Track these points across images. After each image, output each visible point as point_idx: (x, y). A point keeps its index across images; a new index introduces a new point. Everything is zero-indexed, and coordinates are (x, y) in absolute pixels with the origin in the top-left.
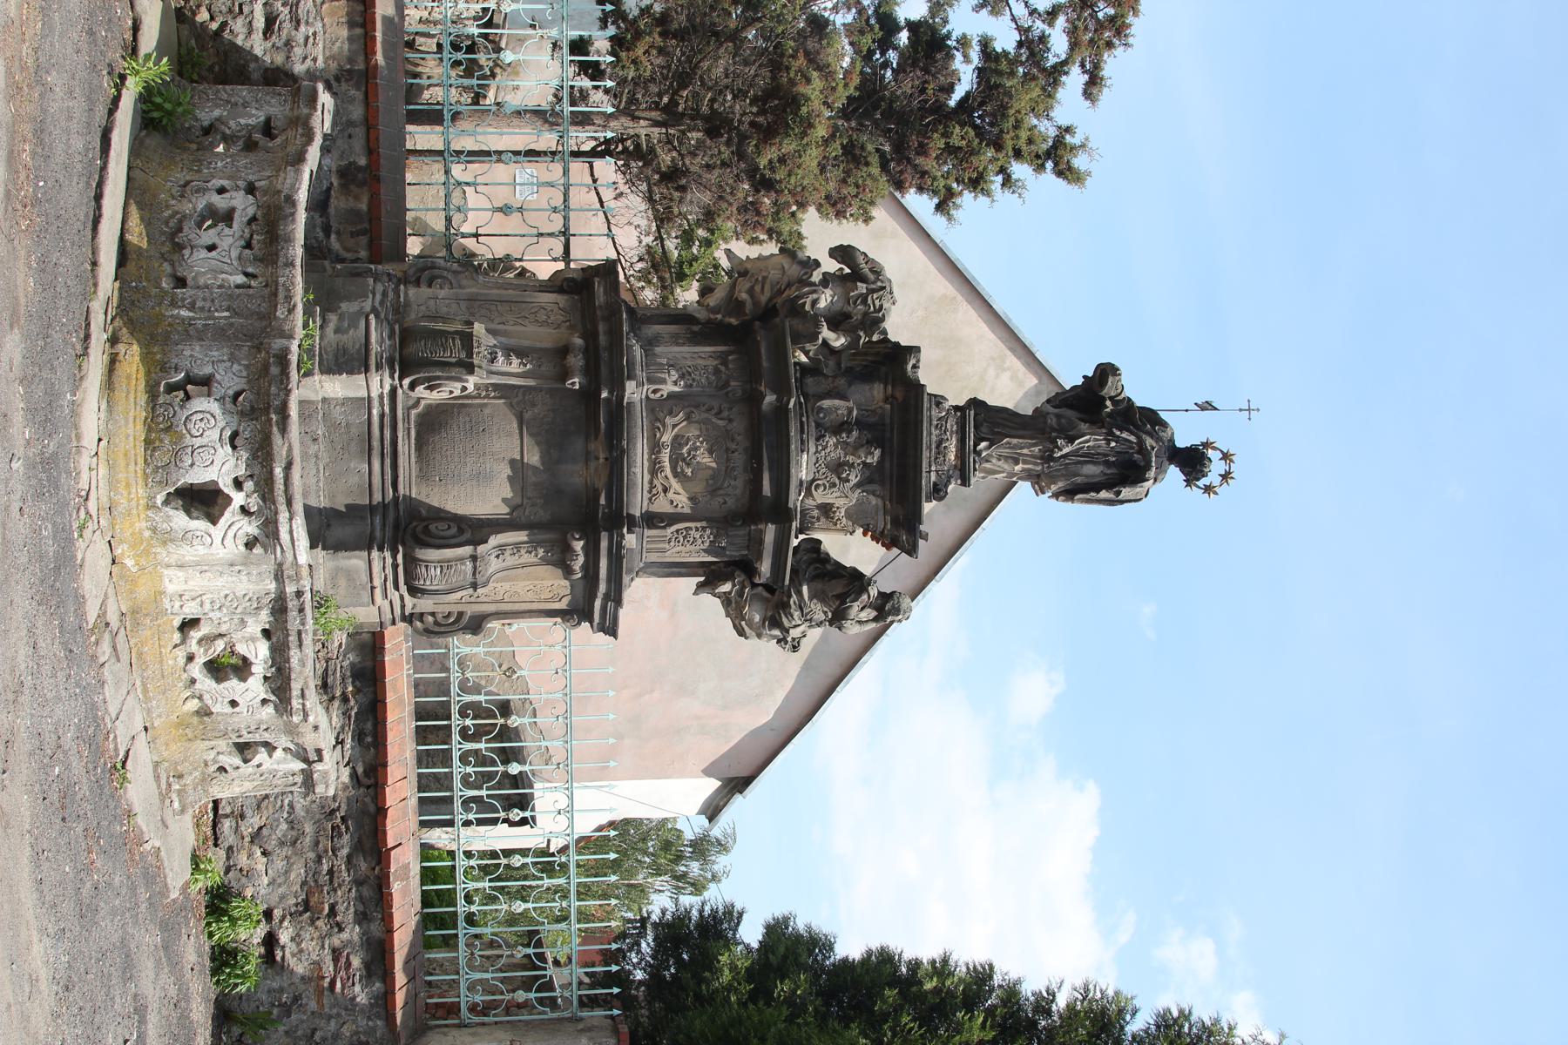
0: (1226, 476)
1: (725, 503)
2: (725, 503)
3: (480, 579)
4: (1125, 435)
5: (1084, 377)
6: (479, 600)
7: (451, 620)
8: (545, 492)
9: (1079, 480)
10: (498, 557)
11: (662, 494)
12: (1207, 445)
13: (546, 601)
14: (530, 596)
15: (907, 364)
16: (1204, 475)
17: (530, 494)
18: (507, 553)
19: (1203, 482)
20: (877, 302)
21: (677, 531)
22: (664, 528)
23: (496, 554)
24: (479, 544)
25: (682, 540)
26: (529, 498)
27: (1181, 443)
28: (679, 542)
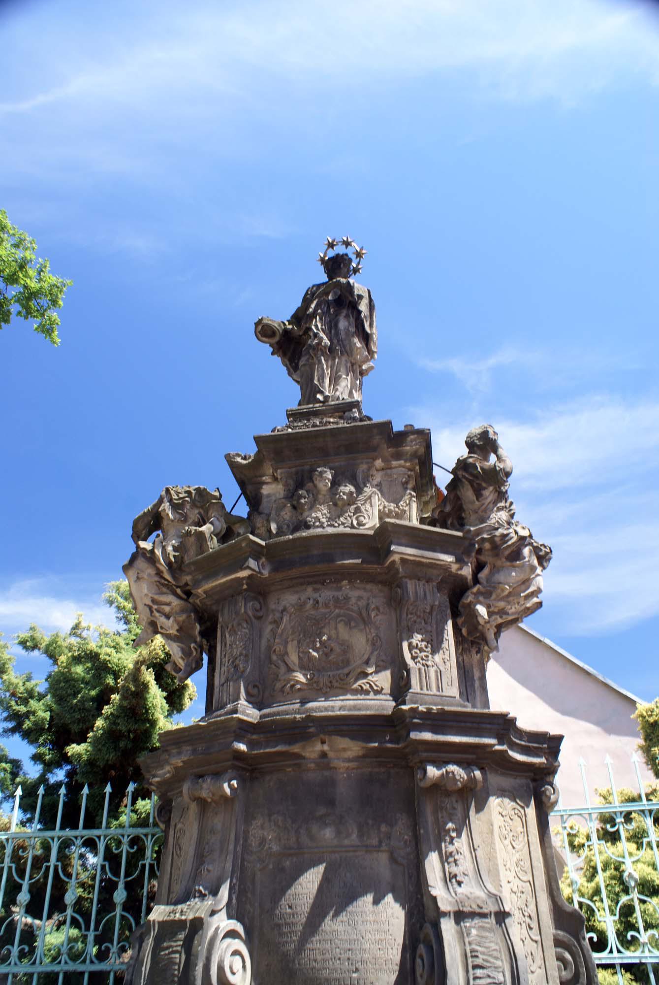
0: (347, 244)
1: (377, 608)
2: (377, 608)
3: (491, 907)
4: (313, 306)
5: (273, 354)
6: (534, 915)
7: (568, 956)
8: (370, 822)
9: (352, 329)
10: (459, 883)
11: (370, 677)
12: (322, 260)
13: (525, 825)
14: (521, 844)
15: (241, 463)
16: (347, 255)
17: (375, 841)
18: (454, 869)
19: (353, 257)
20: (181, 496)
21: (414, 658)
22: (408, 672)
23: (456, 885)
24: (438, 908)
25: (423, 654)
26: (380, 842)
27: (324, 278)
28: (427, 656)
